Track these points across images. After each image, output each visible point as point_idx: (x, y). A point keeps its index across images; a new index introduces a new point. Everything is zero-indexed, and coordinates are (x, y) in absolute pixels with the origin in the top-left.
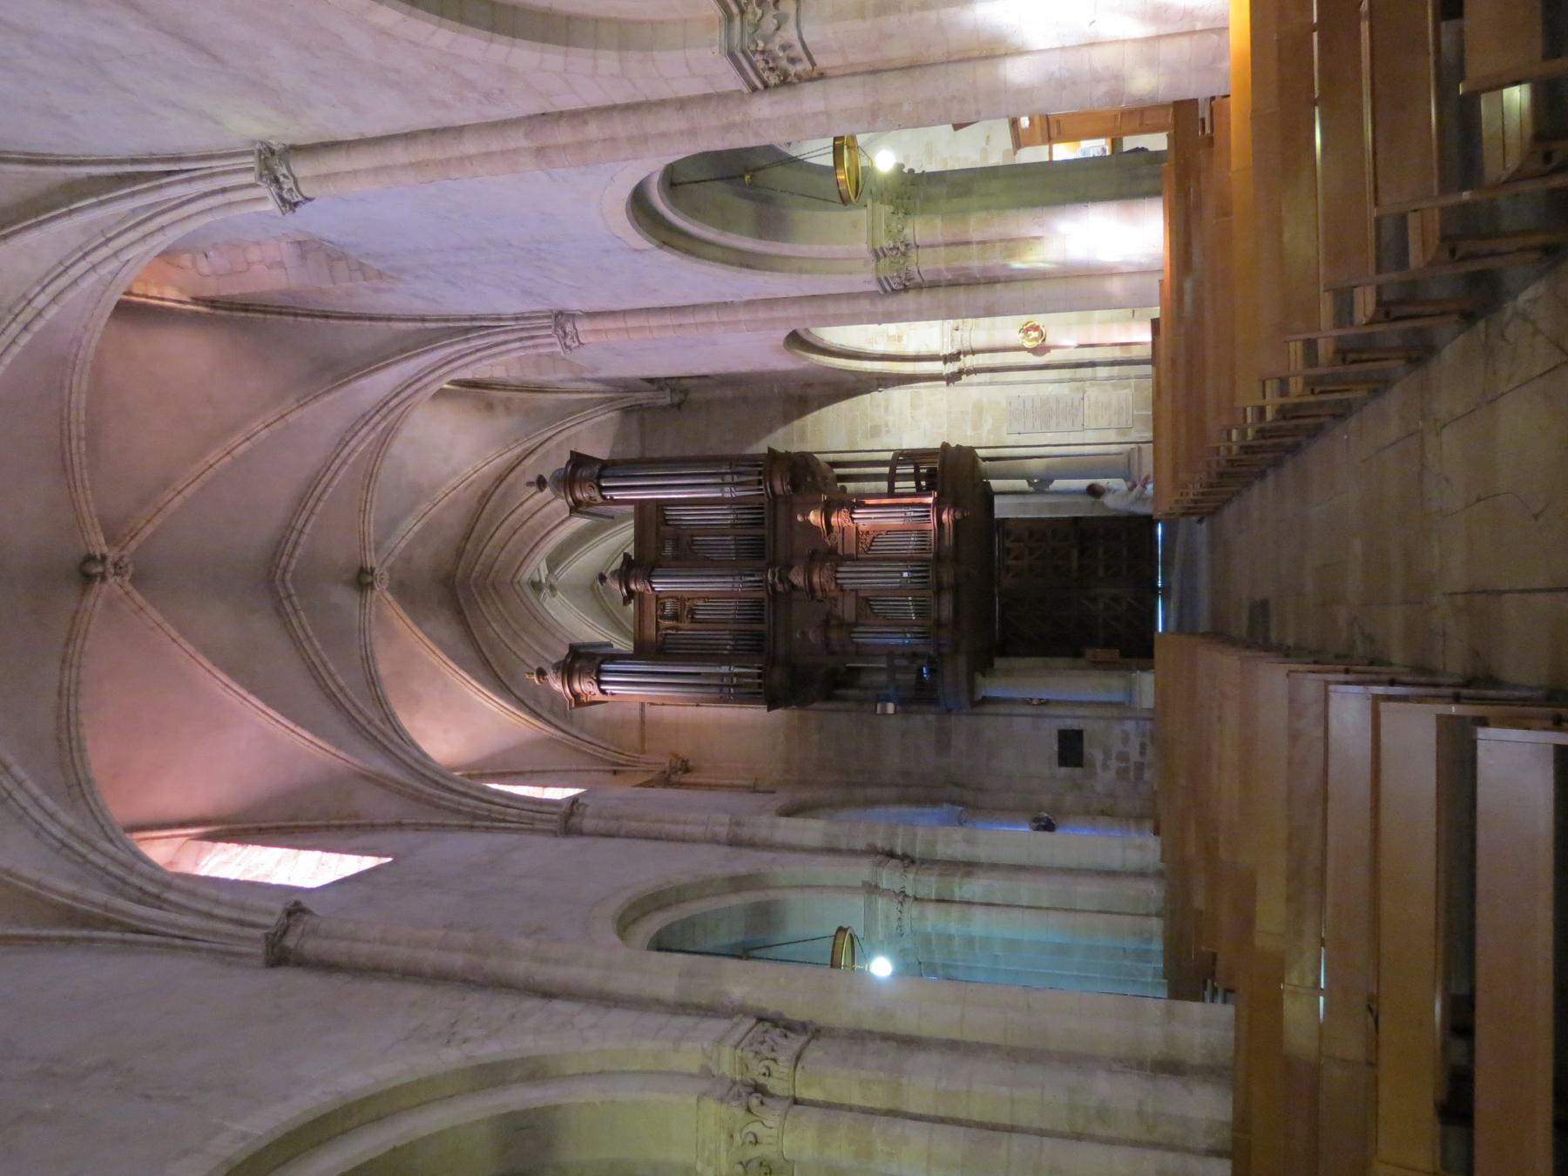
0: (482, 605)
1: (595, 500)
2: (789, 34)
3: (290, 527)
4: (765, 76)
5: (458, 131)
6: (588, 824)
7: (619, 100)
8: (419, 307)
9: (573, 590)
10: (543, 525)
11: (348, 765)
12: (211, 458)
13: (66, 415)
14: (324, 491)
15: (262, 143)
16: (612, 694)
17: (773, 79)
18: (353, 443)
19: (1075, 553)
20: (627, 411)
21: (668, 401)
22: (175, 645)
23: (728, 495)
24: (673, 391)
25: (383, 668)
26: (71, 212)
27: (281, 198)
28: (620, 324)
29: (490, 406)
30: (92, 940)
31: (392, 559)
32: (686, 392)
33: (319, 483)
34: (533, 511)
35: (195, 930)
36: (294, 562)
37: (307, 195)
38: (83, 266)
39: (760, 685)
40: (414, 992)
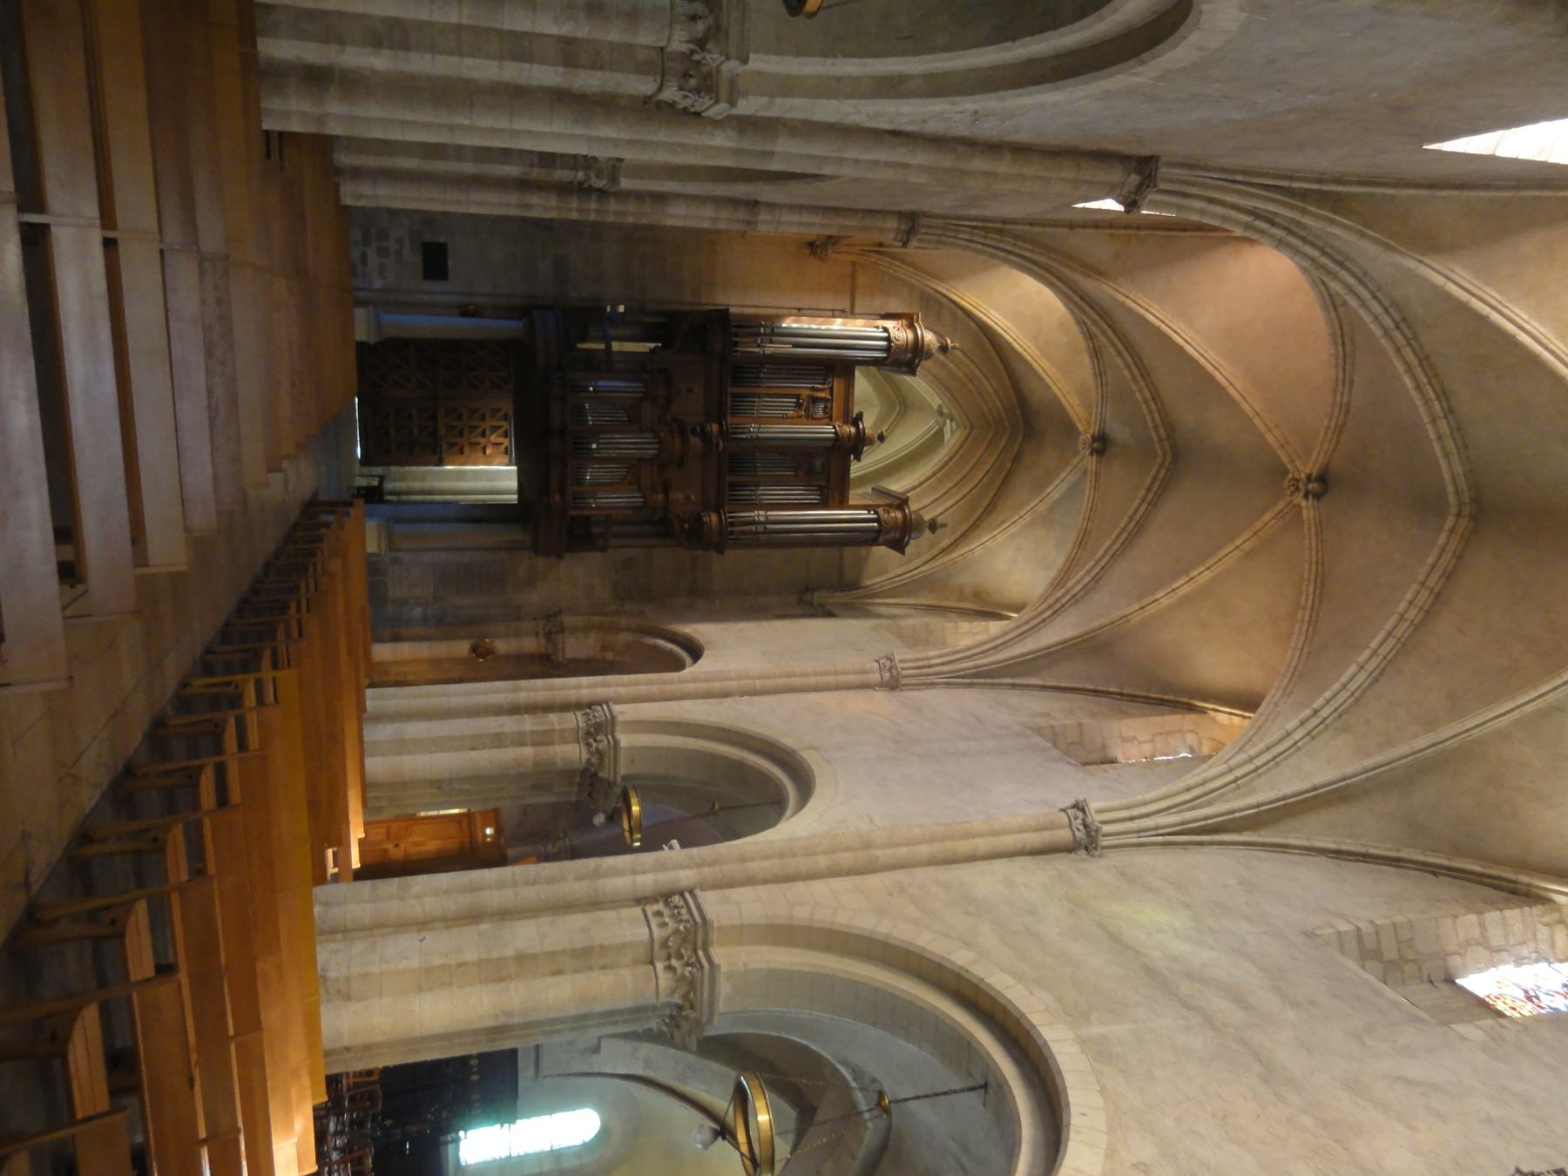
0: (1001, 408)
1: (884, 510)
2: (658, 933)
3: (1153, 505)
4: (682, 902)
6: (891, 224)
7: (801, 885)
8: (1015, 698)
9: (923, 407)
10: (940, 482)
11: (1115, 287)
12: (1208, 575)
13: (1311, 629)
14: (1118, 537)
15: (1093, 856)
16: (877, 327)
17: (676, 899)
18: (1087, 579)
20: (854, 585)
21: (816, 595)
22: (1258, 409)
23: (761, 512)
24: (811, 604)
25: (1086, 360)
26: (1258, 806)
27: (1083, 811)
28: (841, 678)
29: (978, 595)
30: (1320, 181)
31: (1075, 461)
32: (800, 602)
33: (1122, 544)
34: (947, 495)
35: (1224, 190)
36: (1153, 473)
37: (1063, 814)
38: (1258, 762)
39: (736, 335)
40: (1022, 137)
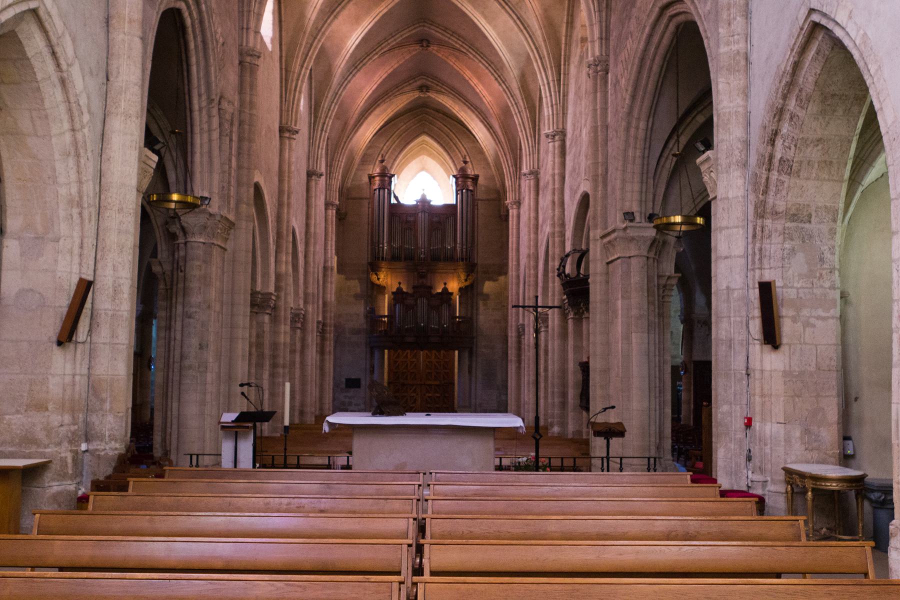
5: (536, 233)
10: (450, 148)
19: (437, 383)
20: (498, 192)
26: (525, 108)
